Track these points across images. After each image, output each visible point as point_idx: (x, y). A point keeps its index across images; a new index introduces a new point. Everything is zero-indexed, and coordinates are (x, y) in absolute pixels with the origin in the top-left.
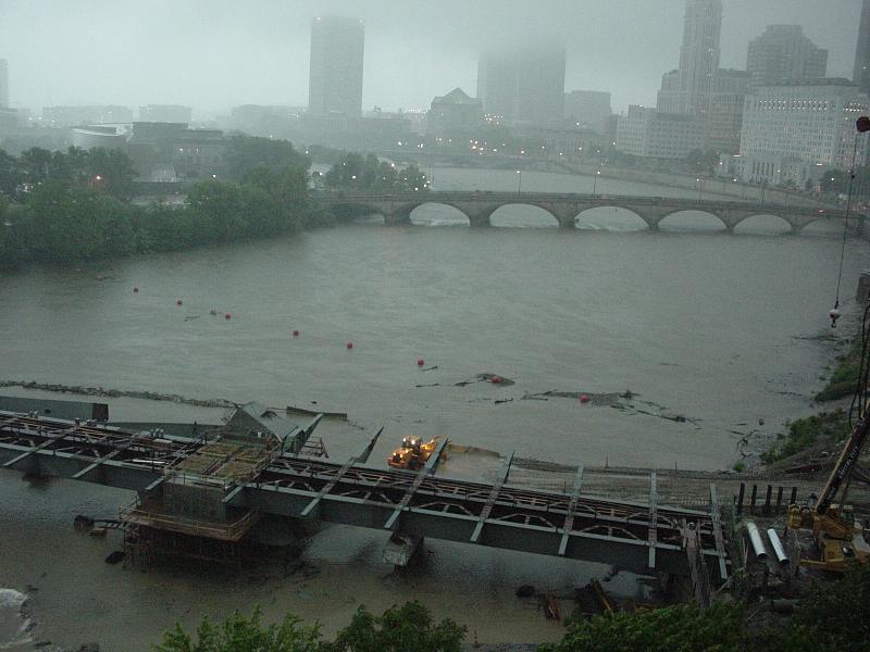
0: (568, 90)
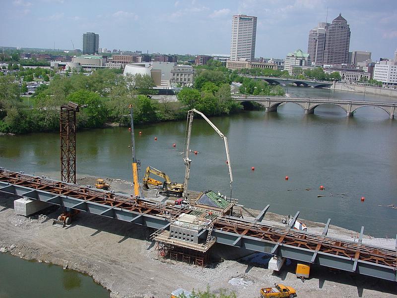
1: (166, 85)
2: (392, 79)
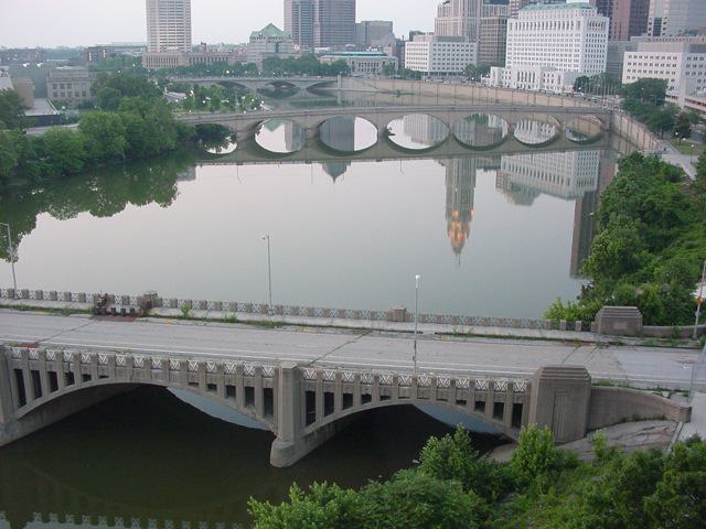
0: (358, 20)
1: (42, 108)
2: (436, 66)
